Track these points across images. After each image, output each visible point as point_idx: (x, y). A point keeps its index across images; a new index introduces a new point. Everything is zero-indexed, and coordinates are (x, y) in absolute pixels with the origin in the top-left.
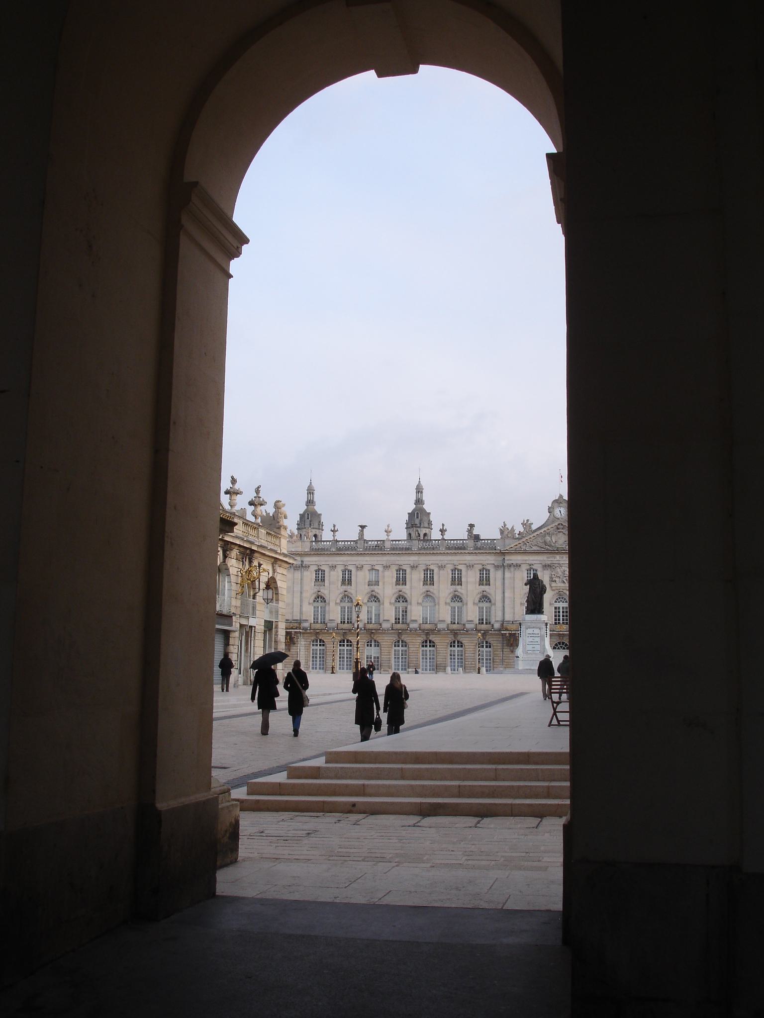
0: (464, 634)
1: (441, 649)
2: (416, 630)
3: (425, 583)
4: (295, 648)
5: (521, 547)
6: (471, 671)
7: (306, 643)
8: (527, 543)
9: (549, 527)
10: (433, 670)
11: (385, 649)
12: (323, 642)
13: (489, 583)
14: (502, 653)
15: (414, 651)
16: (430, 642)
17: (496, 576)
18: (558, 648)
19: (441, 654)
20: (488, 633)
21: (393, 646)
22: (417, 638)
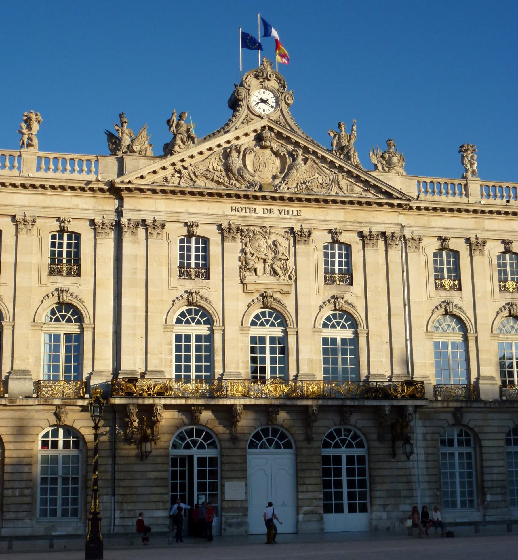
5: (166, 179)
6: (21, 515)
8: (183, 171)
9: (240, 133)
13: (79, 269)
14: (110, 461)
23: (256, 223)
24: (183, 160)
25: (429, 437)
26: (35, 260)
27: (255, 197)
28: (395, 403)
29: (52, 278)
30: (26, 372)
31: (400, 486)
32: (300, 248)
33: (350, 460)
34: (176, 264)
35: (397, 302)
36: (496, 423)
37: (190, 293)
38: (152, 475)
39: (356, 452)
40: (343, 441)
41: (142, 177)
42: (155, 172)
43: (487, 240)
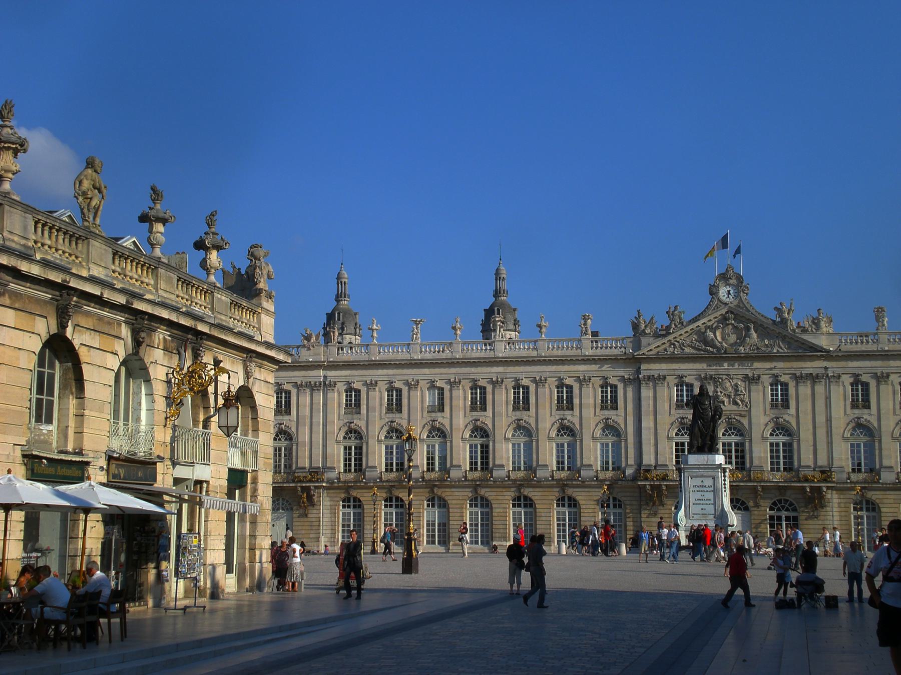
0: (577, 486)
2: (503, 480)
3: (516, 408)
4: (315, 511)
5: (665, 350)
7: (332, 503)
9: (711, 317)
11: (455, 510)
12: (360, 501)
15: (500, 514)
17: (626, 395)
19: (544, 518)
21: (468, 505)
22: (505, 493)
23: (724, 373)
24: (676, 338)
25: (842, 505)
26: (591, 401)
29: (603, 412)
30: (590, 466)
32: (753, 387)
34: (674, 400)
35: (821, 419)
36: (892, 497)
40: (783, 507)
41: (651, 350)
42: (658, 346)
43: (891, 375)
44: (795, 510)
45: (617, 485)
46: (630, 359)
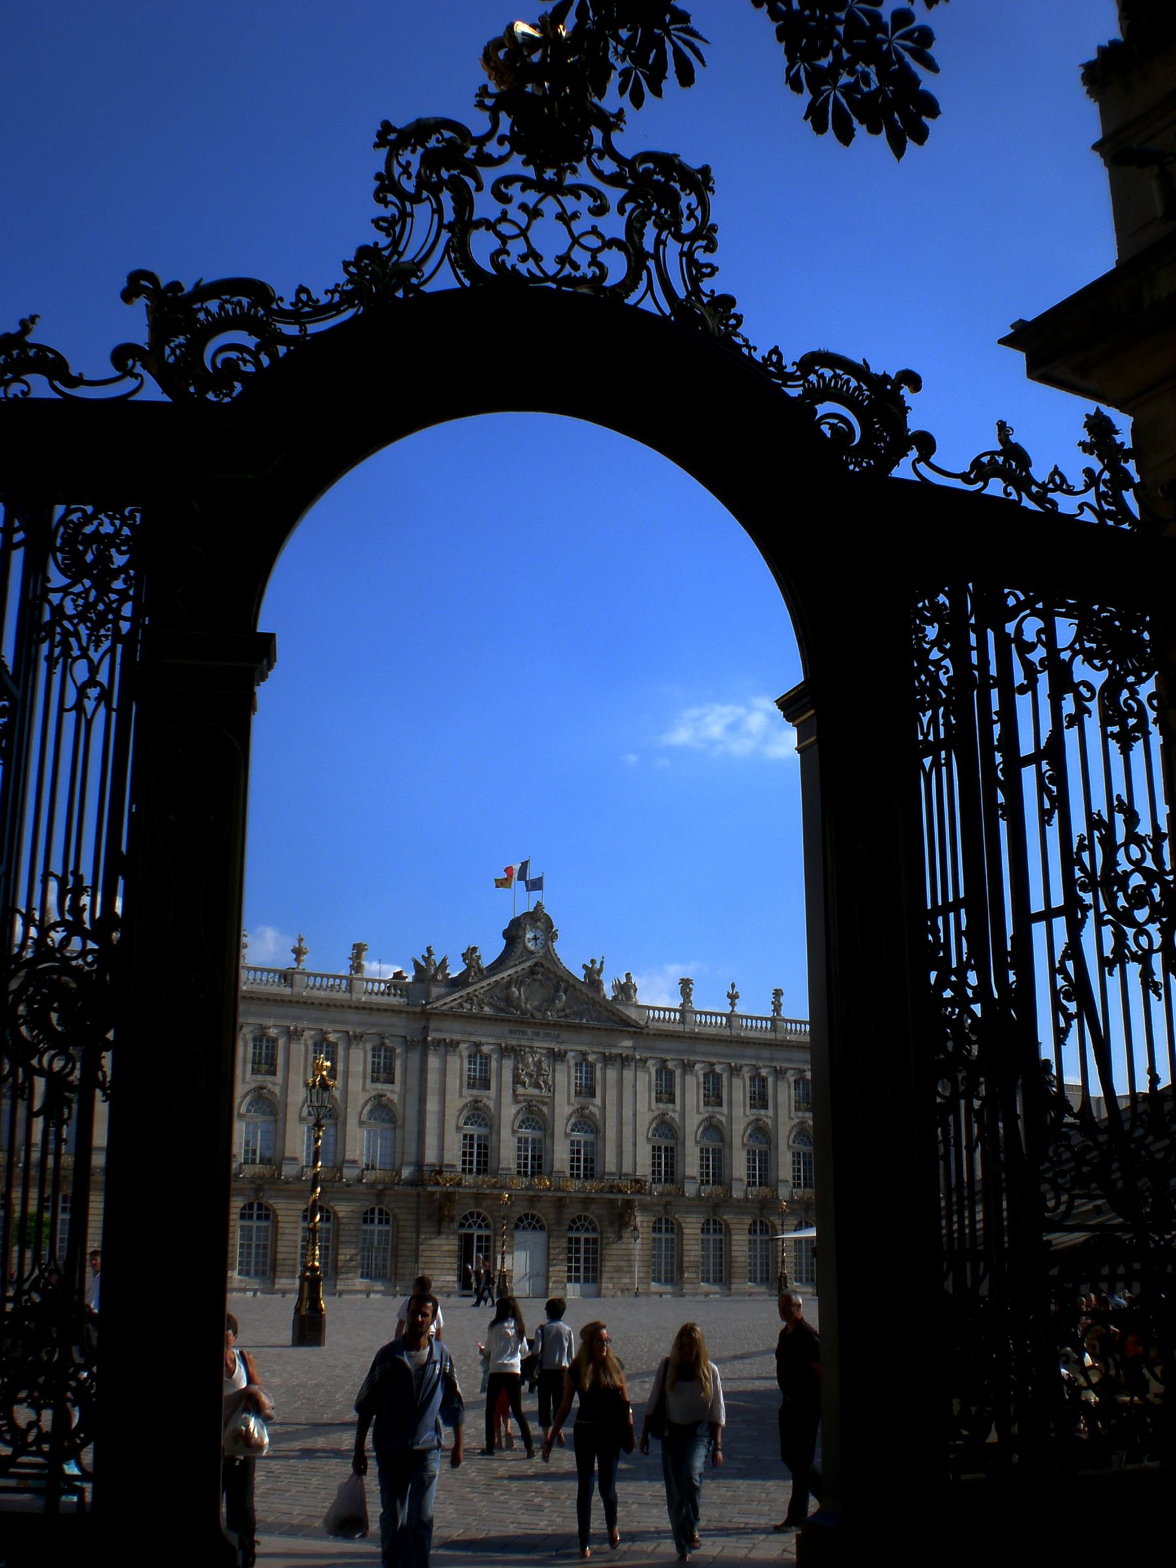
1: (287, 1225)
5: (461, 1005)
10: (264, 1273)
14: (415, 1235)
16: (260, 1207)
18: (524, 1228)
19: (288, 1237)
20: (392, 1189)
25: (645, 1224)
26: (361, 1068)
27: (529, 1023)
28: (626, 1197)
30: (354, 1162)
31: (623, 1263)
32: (559, 1067)
33: (587, 1241)
37: (477, 1102)
38: (446, 1248)
39: (591, 1236)
44: (594, 1230)
45: (390, 1192)
46: (415, 1013)
